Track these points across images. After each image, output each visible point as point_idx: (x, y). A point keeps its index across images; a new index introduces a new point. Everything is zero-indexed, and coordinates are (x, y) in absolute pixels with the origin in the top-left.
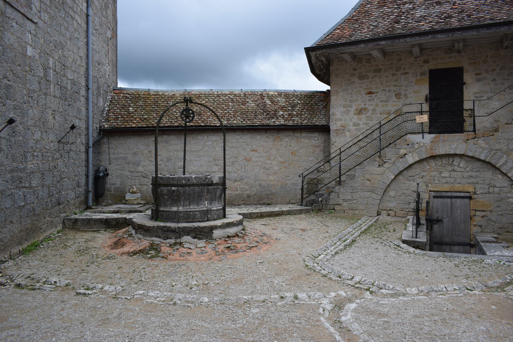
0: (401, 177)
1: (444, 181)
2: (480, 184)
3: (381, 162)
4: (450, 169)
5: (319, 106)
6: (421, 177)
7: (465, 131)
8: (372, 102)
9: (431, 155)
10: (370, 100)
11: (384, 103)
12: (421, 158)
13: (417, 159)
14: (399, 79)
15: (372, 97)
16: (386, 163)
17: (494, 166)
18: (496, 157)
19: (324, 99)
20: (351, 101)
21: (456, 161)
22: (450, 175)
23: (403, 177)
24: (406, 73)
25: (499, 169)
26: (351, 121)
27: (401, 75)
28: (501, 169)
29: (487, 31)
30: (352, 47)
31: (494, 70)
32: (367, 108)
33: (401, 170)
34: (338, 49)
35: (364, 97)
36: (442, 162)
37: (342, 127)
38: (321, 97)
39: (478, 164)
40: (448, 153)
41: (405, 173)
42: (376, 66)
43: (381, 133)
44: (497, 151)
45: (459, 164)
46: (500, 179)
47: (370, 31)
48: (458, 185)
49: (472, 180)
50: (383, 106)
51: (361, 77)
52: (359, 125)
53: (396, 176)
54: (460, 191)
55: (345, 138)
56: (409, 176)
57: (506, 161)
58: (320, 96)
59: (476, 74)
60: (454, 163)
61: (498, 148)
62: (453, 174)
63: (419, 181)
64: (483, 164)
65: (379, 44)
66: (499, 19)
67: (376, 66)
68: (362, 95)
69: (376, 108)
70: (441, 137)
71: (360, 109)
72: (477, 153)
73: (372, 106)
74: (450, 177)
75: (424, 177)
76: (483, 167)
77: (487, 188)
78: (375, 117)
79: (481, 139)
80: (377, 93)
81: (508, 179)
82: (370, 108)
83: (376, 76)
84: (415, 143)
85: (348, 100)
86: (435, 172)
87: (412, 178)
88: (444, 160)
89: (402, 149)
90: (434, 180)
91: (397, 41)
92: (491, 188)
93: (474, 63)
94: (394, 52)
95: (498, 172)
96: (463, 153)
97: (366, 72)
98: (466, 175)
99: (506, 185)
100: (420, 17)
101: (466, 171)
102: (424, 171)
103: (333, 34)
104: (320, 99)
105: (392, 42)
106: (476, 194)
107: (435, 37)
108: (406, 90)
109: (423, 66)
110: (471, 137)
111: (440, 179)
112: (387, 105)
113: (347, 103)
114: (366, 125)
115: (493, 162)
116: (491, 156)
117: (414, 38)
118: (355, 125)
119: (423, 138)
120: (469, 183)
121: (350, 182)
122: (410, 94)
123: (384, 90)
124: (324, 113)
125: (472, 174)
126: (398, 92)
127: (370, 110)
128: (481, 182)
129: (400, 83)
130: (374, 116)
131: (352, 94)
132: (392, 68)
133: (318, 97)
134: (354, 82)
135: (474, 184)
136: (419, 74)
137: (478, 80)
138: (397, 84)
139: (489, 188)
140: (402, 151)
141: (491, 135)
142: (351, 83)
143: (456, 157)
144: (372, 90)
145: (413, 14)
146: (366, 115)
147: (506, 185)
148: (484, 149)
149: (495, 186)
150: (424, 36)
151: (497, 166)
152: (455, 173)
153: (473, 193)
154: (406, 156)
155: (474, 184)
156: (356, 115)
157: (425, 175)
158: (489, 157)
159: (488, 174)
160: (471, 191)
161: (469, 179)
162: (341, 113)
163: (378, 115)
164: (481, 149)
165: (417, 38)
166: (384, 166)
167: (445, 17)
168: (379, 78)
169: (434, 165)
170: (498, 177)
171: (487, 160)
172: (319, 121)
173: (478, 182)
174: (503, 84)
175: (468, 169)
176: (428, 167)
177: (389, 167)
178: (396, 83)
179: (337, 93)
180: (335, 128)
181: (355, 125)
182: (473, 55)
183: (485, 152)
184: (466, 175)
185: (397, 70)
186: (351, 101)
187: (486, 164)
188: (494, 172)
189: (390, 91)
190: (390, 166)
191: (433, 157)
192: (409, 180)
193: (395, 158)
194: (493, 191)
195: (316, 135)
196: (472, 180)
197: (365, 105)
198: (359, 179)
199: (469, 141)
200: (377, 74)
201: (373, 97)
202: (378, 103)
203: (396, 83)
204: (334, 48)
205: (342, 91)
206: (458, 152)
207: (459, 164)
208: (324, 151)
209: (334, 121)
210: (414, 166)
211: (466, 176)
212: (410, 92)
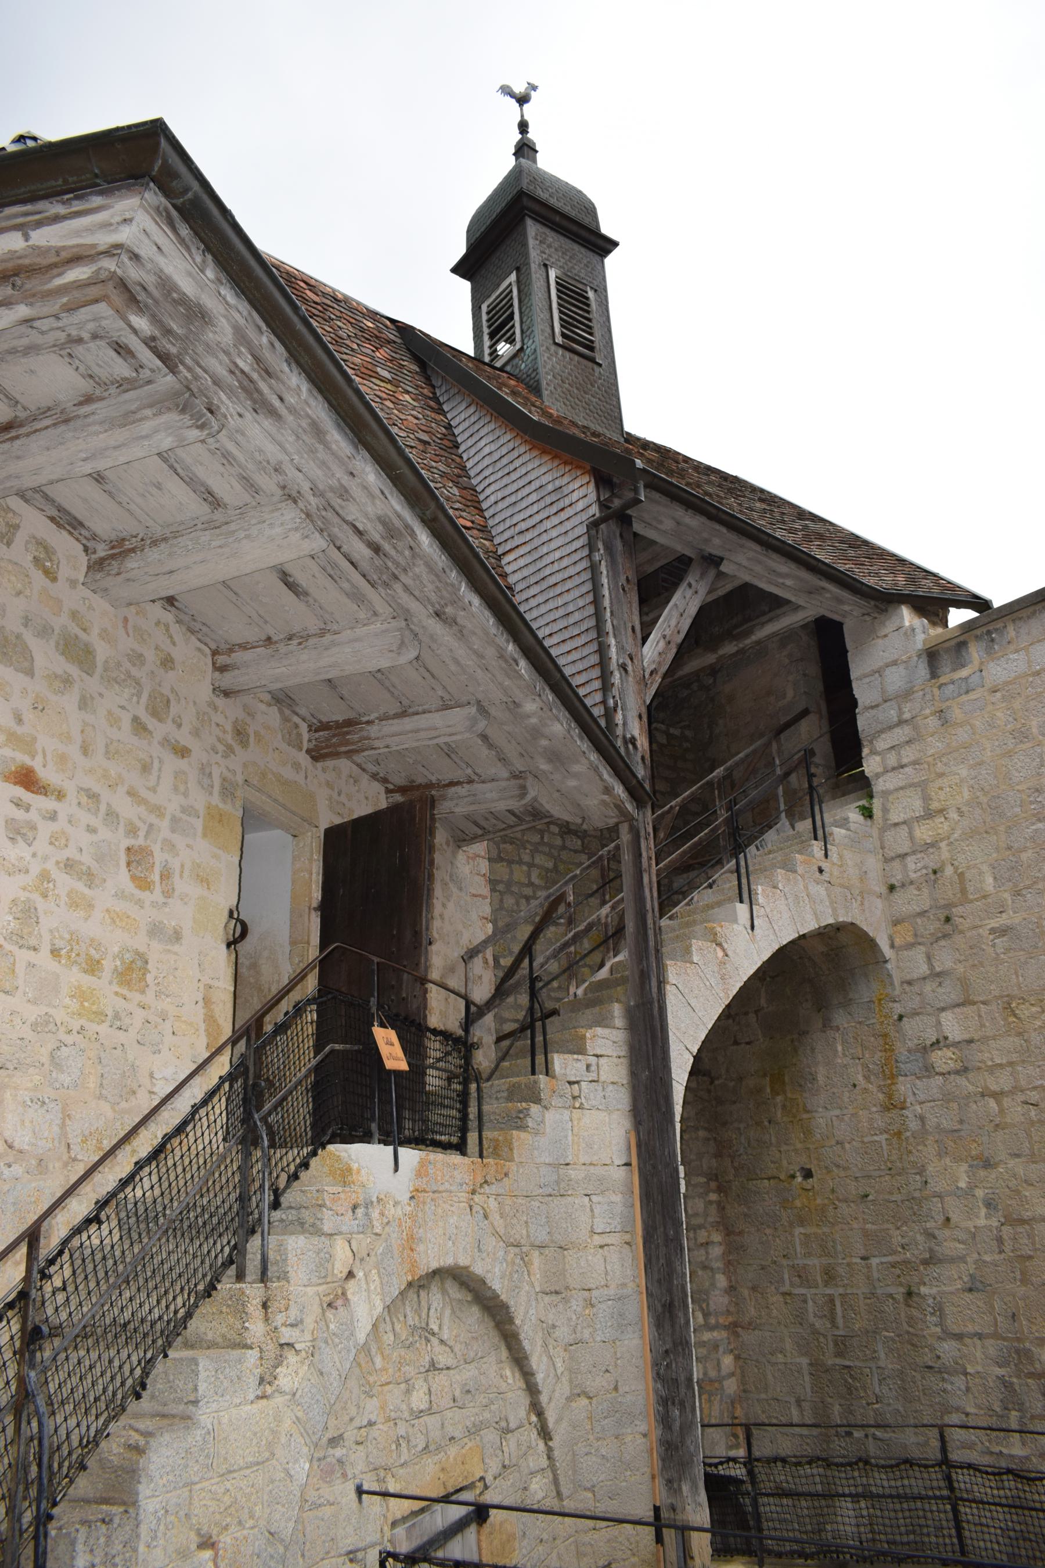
73: (21, 879)
80: (60, 795)
84: (374, 1199)
119: (396, 1169)
126: (140, 841)
129: (153, 790)
130: (24, 956)
144: (37, 764)
168: (84, 703)
201: (33, 816)
202: (50, 866)
212: (182, 866)
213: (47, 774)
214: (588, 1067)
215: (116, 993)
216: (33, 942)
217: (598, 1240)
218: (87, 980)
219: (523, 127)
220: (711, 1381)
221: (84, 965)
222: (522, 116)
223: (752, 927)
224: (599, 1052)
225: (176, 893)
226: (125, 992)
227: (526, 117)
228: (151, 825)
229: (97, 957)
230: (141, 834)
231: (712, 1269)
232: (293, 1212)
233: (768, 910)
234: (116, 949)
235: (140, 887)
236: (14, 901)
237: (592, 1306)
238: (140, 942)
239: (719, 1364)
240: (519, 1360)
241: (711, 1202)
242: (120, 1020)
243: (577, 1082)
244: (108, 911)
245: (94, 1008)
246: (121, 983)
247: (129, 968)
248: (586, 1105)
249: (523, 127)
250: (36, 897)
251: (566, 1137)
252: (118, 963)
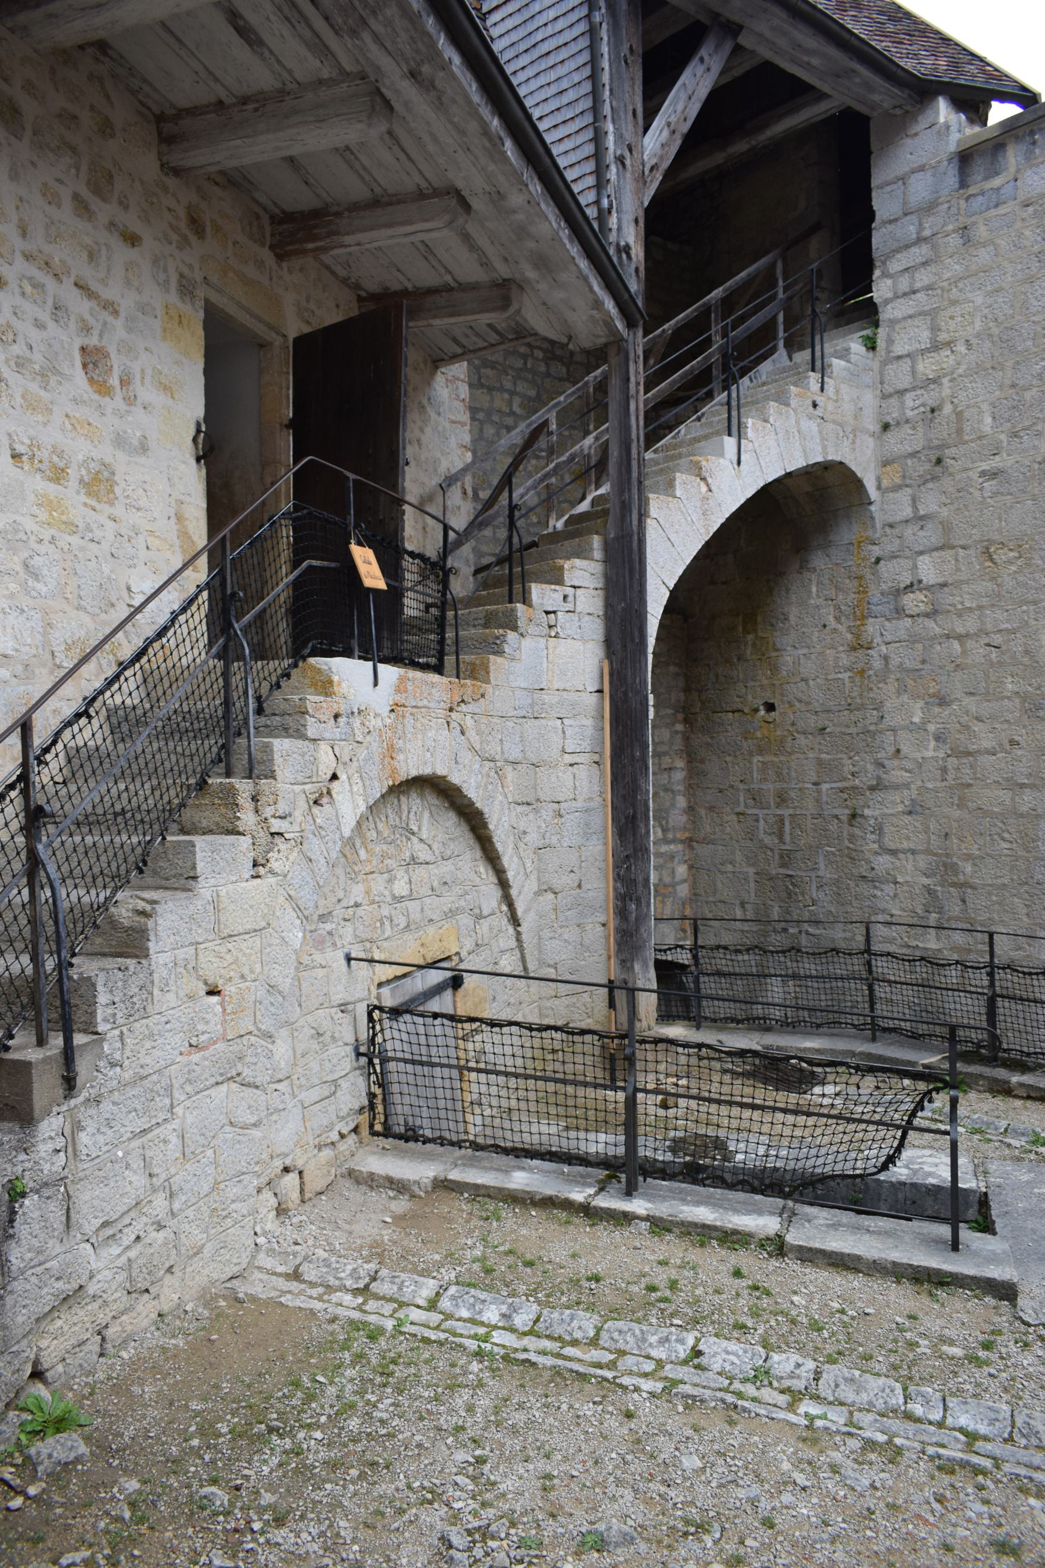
14: (104, 252)
50: (31, 405)
84: (356, 710)
119: (376, 684)
129: (103, 282)
178: (90, 275)
203: (90, 275)
212: (143, 371)
214: (565, 597)
215: (85, 505)
217: (568, 759)
218: (52, 489)
220: (665, 886)
221: (48, 473)
223: (739, 463)
225: (139, 401)
226: (94, 503)
229: (61, 465)
230: (96, 332)
231: (673, 792)
232: (278, 718)
234: (80, 457)
235: (99, 393)
237: (561, 816)
238: (105, 452)
239: (673, 872)
240: (492, 857)
241: (677, 732)
242: (91, 531)
243: (554, 612)
244: (67, 416)
245: (64, 518)
246: (89, 494)
247: (96, 478)
248: (561, 635)
251: (541, 664)
252: (84, 472)
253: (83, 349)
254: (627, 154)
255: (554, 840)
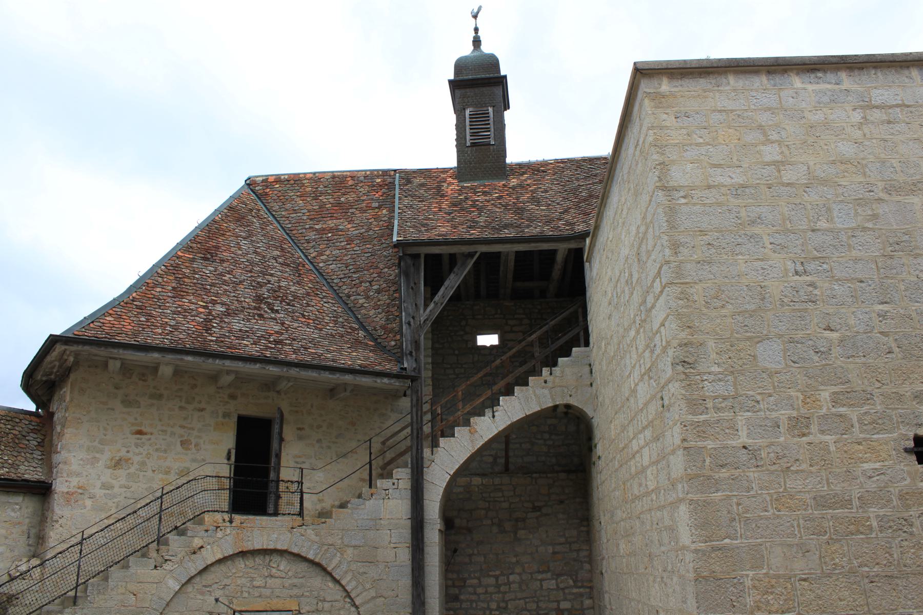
0: (189, 588)
1: (257, 594)
2: (306, 596)
3: (160, 560)
4: (266, 574)
5: (28, 440)
6: (222, 587)
7: (279, 514)
8: (141, 450)
9: (240, 550)
10: (137, 445)
11: (162, 454)
12: (226, 555)
13: (219, 556)
14: (190, 416)
15: (141, 439)
16: (168, 562)
17: (324, 569)
18: (327, 555)
19: (39, 428)
20: (102, 442)
21: (276, 558)
22: (266, 583)
23: (194, 587)
24: (202, 410)
25: (330, 574)
26: (99, 479)
27: (193, 410)
28: (334, 574)
29: (330, 376)
30: (136, 354)
31: (319, 427)
32: (130, 459)
33: (192, 575)
34: (112, 350)
35: (127, 438)
36: (255, 561)
37: (79, 488)
38: (33, 424)
39: (304, 566)
40: (265, 547)
41: (198, 579)
42: (154, 388)
43: (163, 507)
44: (330, 547)
45: (278, 566)
46: (331, 589)
47: (168, 334)
48: (275, 601)
49: (295, 591)
51: (128, 402)
52: (113, 487)
53: (183, 585)
54: (278, 609)
55: (82, 511)
56: (204, 586)
57: (340, 561)
58: (31, 421)
59: (299, 429)
60: (272, 564)
61: (331, 543)
62: (270, 581)
63: (218, 593)
64: (310, 565)
65: (182, 359)
66: (343, 364)
67: (154, 388)
68: (124, 434)
69: (147, 461)
70: (257, 522)
71: (117, 458)
72: (304, 549)
73: (140, 456)
74: (265, 587)
75: (227, 587)
76: (309, 570)
77: (315, 603)
78: (144, 476)
79: (311, 527)
80: (151, 434)
81: (341, 588)
82: (137, 459)
83: (152, 405)
85: (97, 440)
86: (243, 579)
87: (208, 589)
88: (257, 559)
89: (196, 538)
90: (242, 592)
91: (210, 360)
92: (320, 603)
93: (297, 412)
94: (186, 372)
95: (329, 578)
96: (285, 548)
97: (137, 395)
98: (288, 583)
99: (338, 597)
100: (240, 330)
101: (287, 577)
102: (228, 577)
103: (101, 321)
104: (32, 427)
105: (204, 361)
106: (301, 613)
107: (264, 368)
108: (200, 437)
109: (227, 402)
110: (296, 524)
111: (251, 590)
112: (166, 458)
113: (96, 443)
114: (126, 489)
115: (324, 563)
116: (321, 553)
117: (236, 362)
118: (105, 486)
120: (291, 597)
121: (97, 599)
122: (204, 444)
123: (164, 431)
124: (40, 457)
125: (295, 581)
126: (186, 438)
127: (135, 463)
128: (308, 594)
131: (105, 429)
132: (180, 397)
133: (27, 423)
134: (113, 409)
135: (298, 597)
136: (221, 415)
137: (300, 438)
138: (186, 425)
139: (317, 603)
140: (197, 542)
141: (322, 523)
142: (108, 409)
143: (274, 555)
145: (229, 323)
146: (128, 471)
147: (338, 597)
148: (313, 542)
149: (324, 600)
150: (250, 364)
151: (329, 569)
152: (273, 579)
153: (297, 612)
154: (202, 550)
155: (298, 597)
156: (109, 468)
157: (228, 584)
158: (319, 556)
159: (317, 581)
160: (293, 608)
161: (292, 589)
162: (81, 462)
163: (150, 473)
164: (309, 543)
165: (240, 363)
166: (164, 567)
167: (275, 341)
169: (243, 566)
170: (328, 586)
171: (317, 560)
172: (30, 472)
173: (303, 595)
174: (329, 447)
175: (290, 574)
176: (234, 571)
177: (172, 568)
179: (79, 423)
180: (66, 490)
181: (105, 486)
182: (297, 400)
183: (315, 547)
184: (288, 583)
185: (188, 402)
186: (102, 442)
187: (314, 566)
188: (324, 578)
189: (173, 434)
190: (175, 566)
191: (243, 554)
192: (202, 593)
193: (183, 553)
194: (323, 608)
195: (19, 499)
196: (295, 591)
197: (128, 452)
198: (115, 593)
199: (295, 530)
200: (155, 402)
201: (143, 440)
204: (106, 348)
205: (87, 421)
206: (279, 547)
207: (278, 566)
208: (29, 534)
209: (65, 475)
210: (212, 569)
211: (287, 585)
212: (204, 441)
213: (144, 430)
214: (394, 484)
216: (145, 470)
217: (392, 545)
218: (164, 477)
219: (476, 30)
220: (576, 610)
222: (476, 25)
224: (399, 478)
227: (478, 26)
228: (189, 433)
231: (581, 561)
233: (505, 407)
234: (176, 468)
235: (186, 450)
236: (138, 462)
239: (582, 602)
240: (337, 581)
249: (476, 30)
250: (146, 459)
251: (381, 509)
252: (177, 471)
253: (181, 441)
254: (412, 320)
255: (385, 577)
